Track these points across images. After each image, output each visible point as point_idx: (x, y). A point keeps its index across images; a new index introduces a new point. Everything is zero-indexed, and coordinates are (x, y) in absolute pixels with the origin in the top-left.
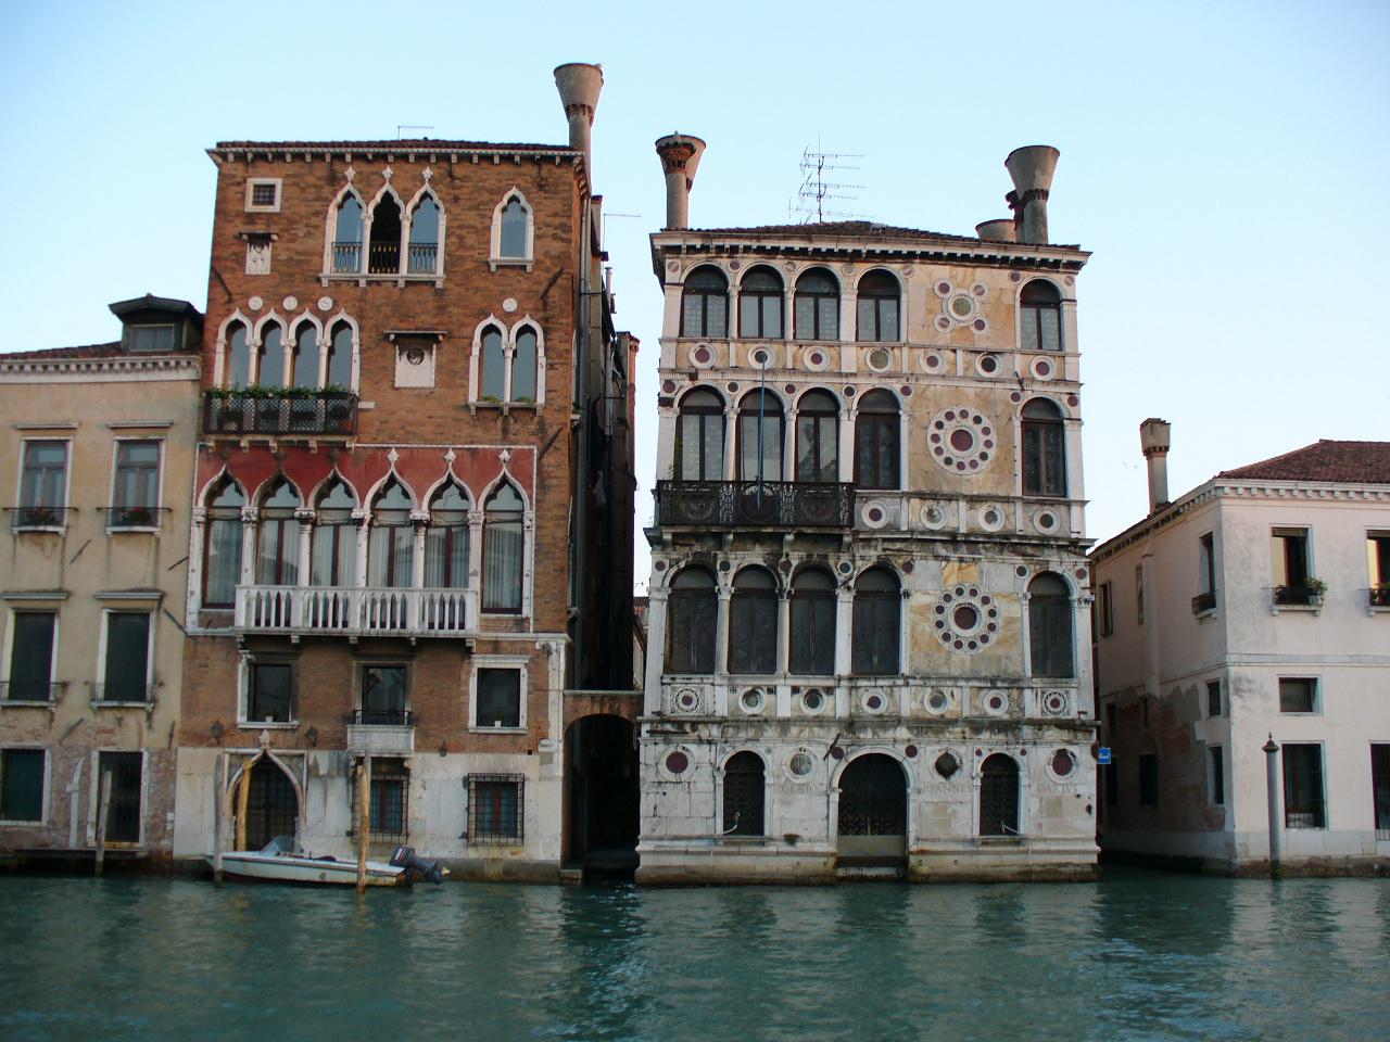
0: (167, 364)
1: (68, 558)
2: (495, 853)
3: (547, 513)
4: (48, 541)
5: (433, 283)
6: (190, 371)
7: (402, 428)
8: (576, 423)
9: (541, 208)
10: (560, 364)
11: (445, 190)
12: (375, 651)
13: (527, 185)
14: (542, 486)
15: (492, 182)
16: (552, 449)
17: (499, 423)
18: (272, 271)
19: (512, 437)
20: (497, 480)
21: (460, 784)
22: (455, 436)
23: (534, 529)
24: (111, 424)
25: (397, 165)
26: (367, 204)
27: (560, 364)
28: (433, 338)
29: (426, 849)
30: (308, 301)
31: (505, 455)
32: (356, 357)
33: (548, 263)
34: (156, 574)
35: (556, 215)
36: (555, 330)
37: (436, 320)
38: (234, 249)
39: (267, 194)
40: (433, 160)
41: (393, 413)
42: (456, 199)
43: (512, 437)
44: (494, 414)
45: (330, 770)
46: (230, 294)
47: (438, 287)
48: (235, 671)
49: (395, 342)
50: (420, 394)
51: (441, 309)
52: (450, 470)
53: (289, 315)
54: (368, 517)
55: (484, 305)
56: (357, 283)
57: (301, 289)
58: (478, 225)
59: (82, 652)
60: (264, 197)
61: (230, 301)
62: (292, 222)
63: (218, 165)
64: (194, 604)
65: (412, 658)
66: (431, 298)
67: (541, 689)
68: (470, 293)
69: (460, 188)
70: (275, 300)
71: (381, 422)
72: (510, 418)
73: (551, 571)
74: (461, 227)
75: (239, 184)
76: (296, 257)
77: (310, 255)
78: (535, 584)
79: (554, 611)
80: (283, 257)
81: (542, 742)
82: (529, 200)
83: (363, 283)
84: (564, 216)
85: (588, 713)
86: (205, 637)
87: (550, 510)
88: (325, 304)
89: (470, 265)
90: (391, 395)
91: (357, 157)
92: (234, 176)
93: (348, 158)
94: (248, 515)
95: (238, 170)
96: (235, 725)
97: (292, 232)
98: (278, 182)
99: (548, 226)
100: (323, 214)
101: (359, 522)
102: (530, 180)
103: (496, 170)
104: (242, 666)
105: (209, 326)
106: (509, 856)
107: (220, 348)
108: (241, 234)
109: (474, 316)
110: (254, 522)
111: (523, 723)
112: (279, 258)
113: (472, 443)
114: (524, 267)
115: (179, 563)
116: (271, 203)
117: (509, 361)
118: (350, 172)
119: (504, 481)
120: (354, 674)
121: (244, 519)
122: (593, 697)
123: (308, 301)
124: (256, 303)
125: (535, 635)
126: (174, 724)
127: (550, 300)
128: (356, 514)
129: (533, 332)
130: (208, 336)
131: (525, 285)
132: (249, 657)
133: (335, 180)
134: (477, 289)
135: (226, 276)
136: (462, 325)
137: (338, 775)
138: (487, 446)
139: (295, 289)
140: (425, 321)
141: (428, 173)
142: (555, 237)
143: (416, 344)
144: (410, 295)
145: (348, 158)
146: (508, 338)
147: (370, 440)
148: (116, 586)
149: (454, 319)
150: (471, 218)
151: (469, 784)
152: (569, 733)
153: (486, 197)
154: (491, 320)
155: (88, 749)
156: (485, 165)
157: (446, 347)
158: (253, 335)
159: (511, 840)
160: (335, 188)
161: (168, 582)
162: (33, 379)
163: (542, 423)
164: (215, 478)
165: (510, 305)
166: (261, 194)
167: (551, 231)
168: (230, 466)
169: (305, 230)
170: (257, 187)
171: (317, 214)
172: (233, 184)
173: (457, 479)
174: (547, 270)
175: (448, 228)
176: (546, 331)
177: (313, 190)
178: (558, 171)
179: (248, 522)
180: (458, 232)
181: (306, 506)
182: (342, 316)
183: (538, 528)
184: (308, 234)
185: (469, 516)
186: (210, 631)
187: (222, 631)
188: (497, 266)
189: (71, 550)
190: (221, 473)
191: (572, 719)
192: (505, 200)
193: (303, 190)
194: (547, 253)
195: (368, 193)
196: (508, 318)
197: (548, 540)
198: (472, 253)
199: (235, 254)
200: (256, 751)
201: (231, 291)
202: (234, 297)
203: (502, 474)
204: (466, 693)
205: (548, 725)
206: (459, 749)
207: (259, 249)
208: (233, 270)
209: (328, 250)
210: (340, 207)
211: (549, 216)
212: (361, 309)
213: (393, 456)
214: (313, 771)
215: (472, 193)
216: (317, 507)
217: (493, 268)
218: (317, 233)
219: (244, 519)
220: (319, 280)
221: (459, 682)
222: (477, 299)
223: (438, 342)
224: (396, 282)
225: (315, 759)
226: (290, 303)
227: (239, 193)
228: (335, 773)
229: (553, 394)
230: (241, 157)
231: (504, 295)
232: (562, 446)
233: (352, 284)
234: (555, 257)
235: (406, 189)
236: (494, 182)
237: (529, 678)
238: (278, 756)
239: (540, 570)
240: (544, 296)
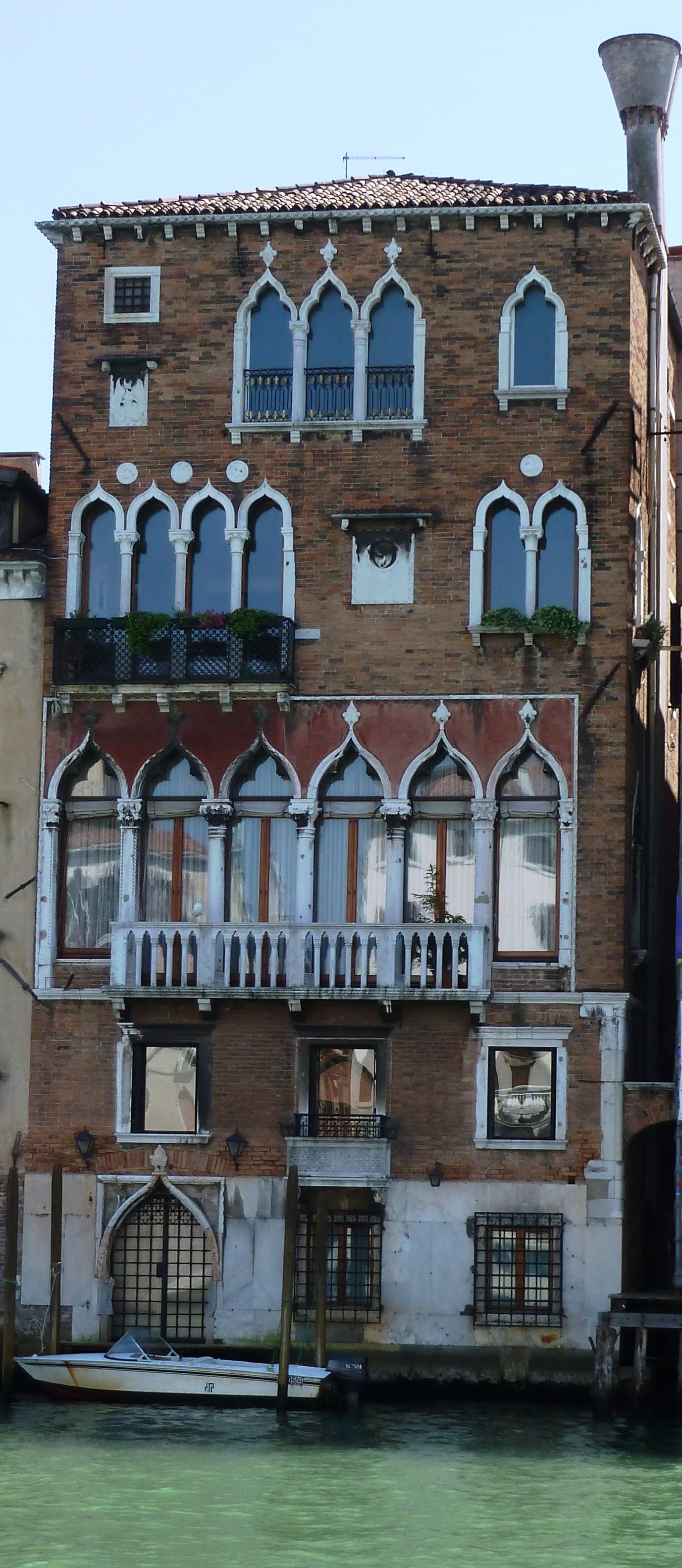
2: (517, 1338)
3: (598, 802)
5: (408, 434)
6: (28, 584)
7: (366, 669)
8: (642, 653)
9: (581, 300)
10: (613, 560)
11: (421, 276)
12: (330, 1021)
13: (556, 263)
14: (587, 758)
15: (498, 261)
16: (604, 698)
17: (519, 658)
18: (151, 419)
19: (540, 681)
20: (516, 750)
21: (464, 1229)
22: (448, 681)
23: (574, 827)
25: (344, 237)
26: (298, 304)
27: (613, 560)
29: (409, 1331)
30: (209, 467)
32: (289, 556)
33: (593, 393)
35: (603, 312)
36: (605, 505)
37: (415, 494)
39: (138, 292)
40: (401, 227)
41: (349, 646)
42: (441, 292)
43: (540, 681)
44: (511, 643)
45: (261, 1206)
46: (87, 460)
47: (415, 439)
48: (111, 1055)
49: (350, 531)
51: (423, 475)
52: (442, 735)
53: (181, 492)
54: (313, 812)
55: (490, 468)
56: (287, 437)
57: (199, 448)
58: (478, 334)
60: (133, 297)
61: (87, 471)
62: (179, 339)
63: (59, 247)
64: (45, 951)
65: (386, 1032)
68: (468, 448)
69: (445, 273)
70: (156, 468)
71: (331, 661)
72: (536, 650)
73: (604, 893)
74: (449, 338)
75: (92, 278)
76: (187, 397)
77: (211, 393)
78: (578, 915)
79: (609, 957)
80: (168, 395)
81: (592, 1163)
82: (559, 289)
84: (616, 313)
86: (65, 1002)
87: (600, 797)
88: (237, 472)
90: (344, 615)
92: (84, 265)
93: (265, 229)
94: (127, 811)
95: (90, 255)
96: (111, 1139)
97: (182, 354)
98: (153, 272)
99: (591, 331)
100: (226, 324)
101: (301, 820)
102: (561, 255)
103: (505, 239)
104: (122, 1047)
105: (55, 510)
106: (539, 1343)
107: (73, 547)
108: (98, 363)
109: (475, 486)
110: (136, 823)
111: (561, 1132)
112: (161, 398)
113: (475, 691)
114: (554, 402)
115: (23, 887)
116: (145, 308)
117: (531, 559)
118: (268, 254)
119: (528, 750)
120: (297, 1060)
121: (120, 818)
123: (209, 467)
124: (127, 473)
125: (578, 995)
126: (19, 1135)
127: (597, 455)
128: (297, 806)
129: (571, 507)
130: (55, 529)
131: (556, 432)
132: (133, 1032)
133: (245, 266)
134: (480, 441)
135: (79, 430)
136: (457, 501)
137: (273, 1215)
138: (500, 697)
139: (188, 449)
141: (393, 250)
142: (603, 350)
143: (384, 534)
144: (375, 455)
145: (265, 229)
146: (529, 522)
147: (316, 689)
149: (443, 492)
150: (465, 322)
151: (477, 1227)
153: (488, 286)
154: (503, 491)
156: (486, 232)
157: (431, 537)
158: (124, 529)
159: (542, 1318)
160: (246, 279)
163: (585, 657)
164: (74, 755)
165: (532, 465)
166: (129, 293)
167: (597, 340)
169: (201, 351)
170: (121, 284)
171: (218, 323)
172: (82, 278)
174: (592, 405)
175: (429, 341)
176: (590, 508)
177: (212, 285)
178: (604, 237)
179: (127, 823)
180: (446, 346)
181: (216, 796)
182: (265, 490)
183: (582, 825)
184: (206, 358)
185: (474, 807)
186: (73, 994)
187: (89, 994)
188: (510, 401)
190: (82, 746)
191: (637, 1127)
192: (519, 294)
193: (195, 284)
194: (590, 375)
195: (296, 286)
196: (530, 488)
197: (598, 844)
198: (469, 382)
199: (91, 394)
200: (146, 1178)
201: (89, 455)
202: (94, 463)
203: (524, 739)
204: (472, 1087)
205: (600, 1137)
206: (462, 1174)
207: (127, 385)
208: (89, 420)
209: (238, 382)
210: (255, 309)
211: (590, 314)
212: (295, 479)
213: (351, 715)
214: (233, 1211)
215: (466, 280)
216: (234, 797)
217: (504, 406)
218: (220, 355)
219: (120, 818)
220: (226, 434)
221: (460, 1069)
222: (480, 457)
223: (418, 530)
224: (348, 433)
225: (237, 1193)
226: (182, 472)
227: (92, 292)
228: (268, 1212)
229: (603, 610)
230: (92, 234)
233: (279, 438)
234: (604, 383)
235: (359, 279)
236: (499, 260)
237: (570, 1063)
238: (177, 1185)
239: (586, 892)
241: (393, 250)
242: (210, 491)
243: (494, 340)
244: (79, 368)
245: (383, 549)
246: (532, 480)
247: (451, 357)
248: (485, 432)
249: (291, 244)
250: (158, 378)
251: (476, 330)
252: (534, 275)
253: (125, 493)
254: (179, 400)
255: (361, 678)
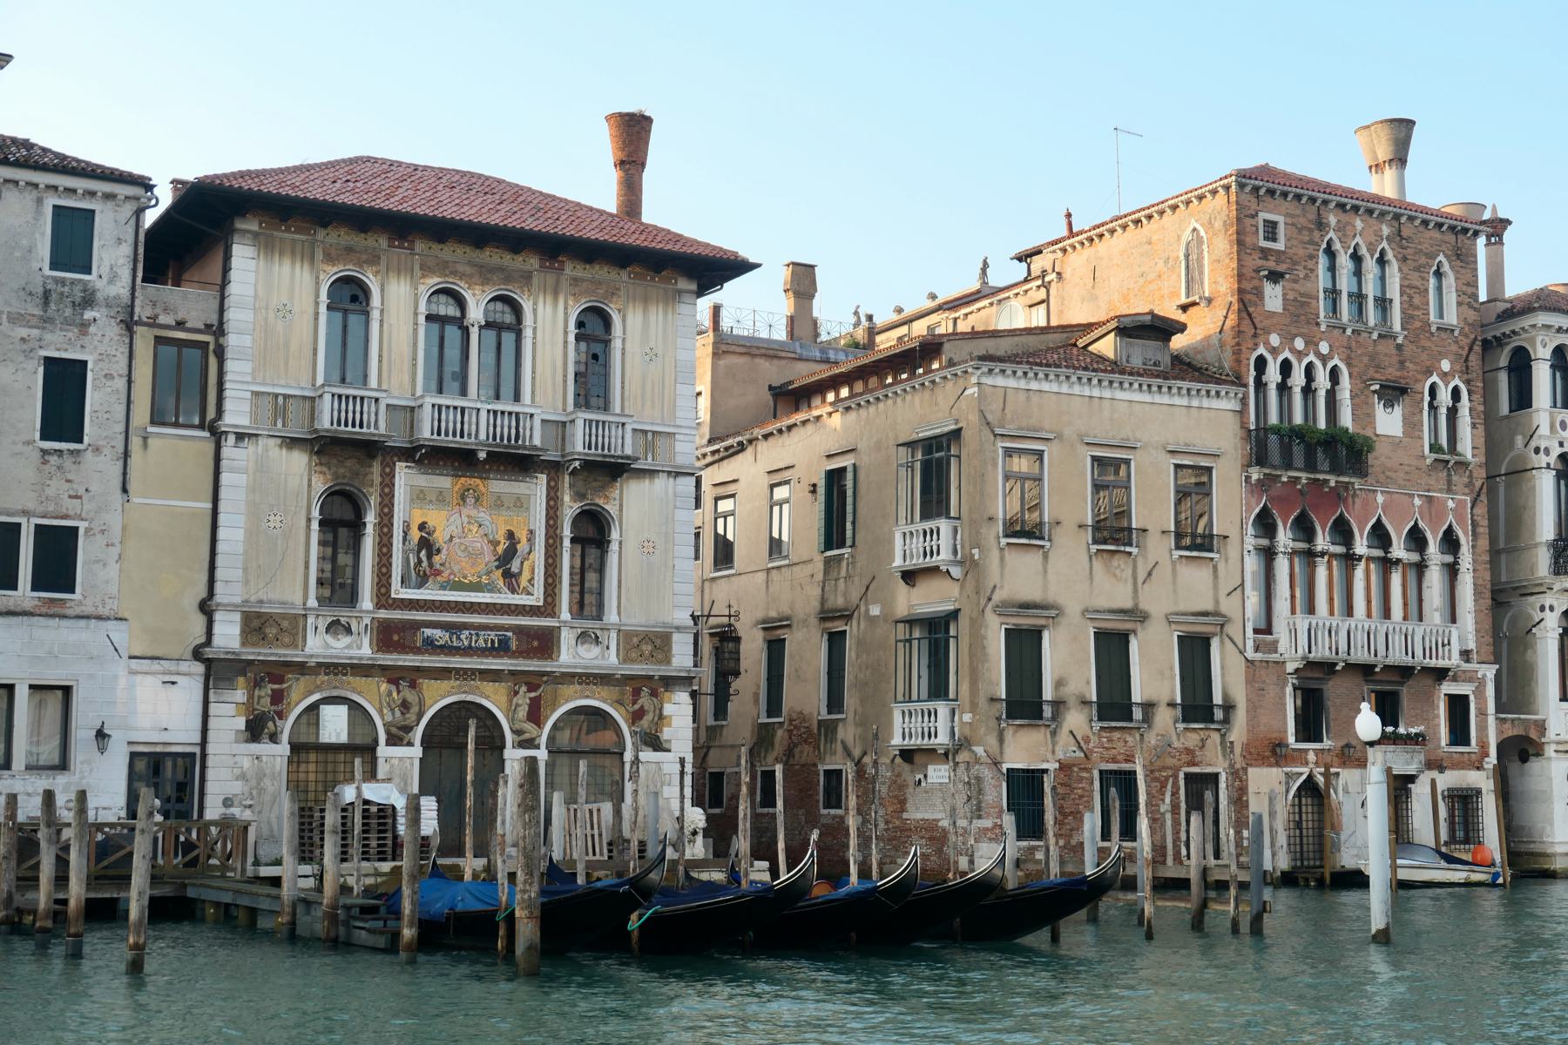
0: (1218, 393)
1: (1140, 581)
4: (1117, 561)
14: (1474, 531)
24: (1170, 448)
28: (1403, 391)
30: (1311, 343)
31: (1451, 504)
34: (1217, 602)
35: (1468, 284)
38: (1256, 282)
48: (1283, 697)
50: (1395, 443)
51: (1402, 363)
53: (1300, 355)
59: (1153, 674)
61: (1255, 335)
62: (1295, 263)
65: (1402, 684)
66: (1394, 352)
67: (1482, 713)
70: (1289, 339)
80: (1290, 297)
82: (1452, 267)
83: (1349, 332)
85: (1510, 734)
88: (1324, 348)
89: (1418, 324)
91: (1341, 206)
100: (1312, 257)
104: (1289, 689)
111: (1473, 741)
118: (1332, 220)
122: (1513, 720)
123: (1311, 343)
133: (1321, 225)
136: (1417, 381)
140: (1392, 373)
143: (1393, 392)
146: (1444, 397)
148: (1183, 606)
152: (1500, 747)
153: (1423, 260)
155: (1178, 770)
161: (1228, 606)
162: (1096, 393)
163: (1471, 476)
168: (1270, 499)
173: (1420, 523)
174: (1466, 336)
182: (1336, 361)
189: (1141, 576)
196: (1445, 376)
199: (1255, 288)
204: (1438, 716)
208: (1256, 305)
212: (1349, 357)
213: (1380, 499)
217: (1433, 329)
220: (1318, 324)
222: (1424, 357)
231: (1442, 355)
232: (1483, 497)
240: (1466, 360)
241: (1386, 230)
242: (1312, 358)
243: (1427, 290)
244: (1248, 272)
245: (1389, 404)
246: (1445, 374)
247: (1411, 297)
248: (1427, 344)
249: (1345, 218)
250: (1289, 285)
251: (1418, 283)
252: (1441, 258)
253: (1274, 351)
254: (1295, 300)
255: (1382, 478)
